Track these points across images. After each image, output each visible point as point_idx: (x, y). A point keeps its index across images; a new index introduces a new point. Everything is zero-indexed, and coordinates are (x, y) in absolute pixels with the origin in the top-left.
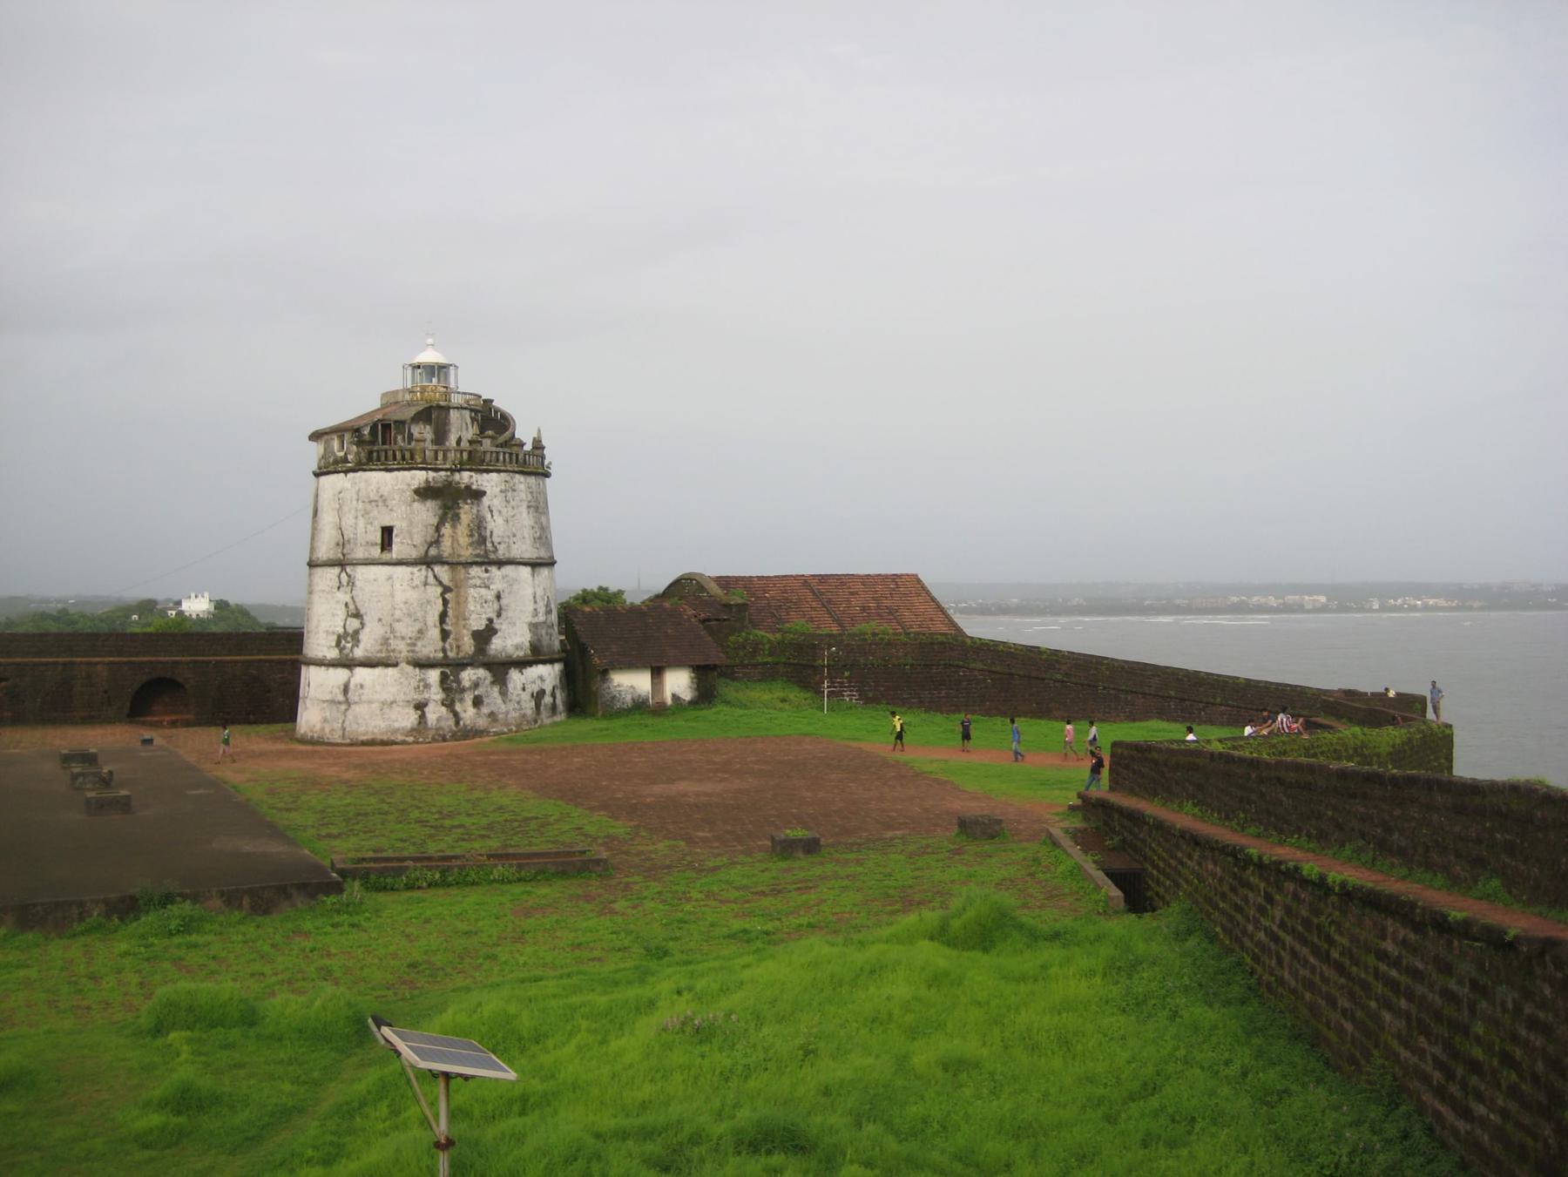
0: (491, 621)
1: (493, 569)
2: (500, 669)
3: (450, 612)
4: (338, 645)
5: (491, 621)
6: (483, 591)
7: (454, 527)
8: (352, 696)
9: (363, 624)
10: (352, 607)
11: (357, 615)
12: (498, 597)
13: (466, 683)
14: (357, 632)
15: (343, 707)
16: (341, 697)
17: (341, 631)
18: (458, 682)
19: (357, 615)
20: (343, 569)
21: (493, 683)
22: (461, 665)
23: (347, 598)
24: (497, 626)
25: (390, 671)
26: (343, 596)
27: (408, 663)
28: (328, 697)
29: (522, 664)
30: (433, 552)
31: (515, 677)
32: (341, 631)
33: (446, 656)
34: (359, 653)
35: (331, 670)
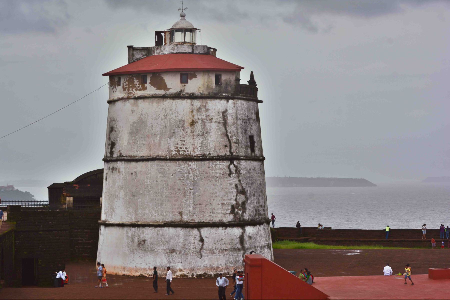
4: (233, 212)
8: (247, 245)
9: (247, 199)
10: (240, 188)
11: (243, 192)
14: (244, 204)
15: (242, 252)
16: (239, 246)
17: (234, 203)
19: (243, 192)
20: (232, 163)
23: (237, 182)
25: (262, 228)
26: (234, 180)
28: (229, 247)
32: (234, 203)
34: (246, 217)
35: (229, 230)
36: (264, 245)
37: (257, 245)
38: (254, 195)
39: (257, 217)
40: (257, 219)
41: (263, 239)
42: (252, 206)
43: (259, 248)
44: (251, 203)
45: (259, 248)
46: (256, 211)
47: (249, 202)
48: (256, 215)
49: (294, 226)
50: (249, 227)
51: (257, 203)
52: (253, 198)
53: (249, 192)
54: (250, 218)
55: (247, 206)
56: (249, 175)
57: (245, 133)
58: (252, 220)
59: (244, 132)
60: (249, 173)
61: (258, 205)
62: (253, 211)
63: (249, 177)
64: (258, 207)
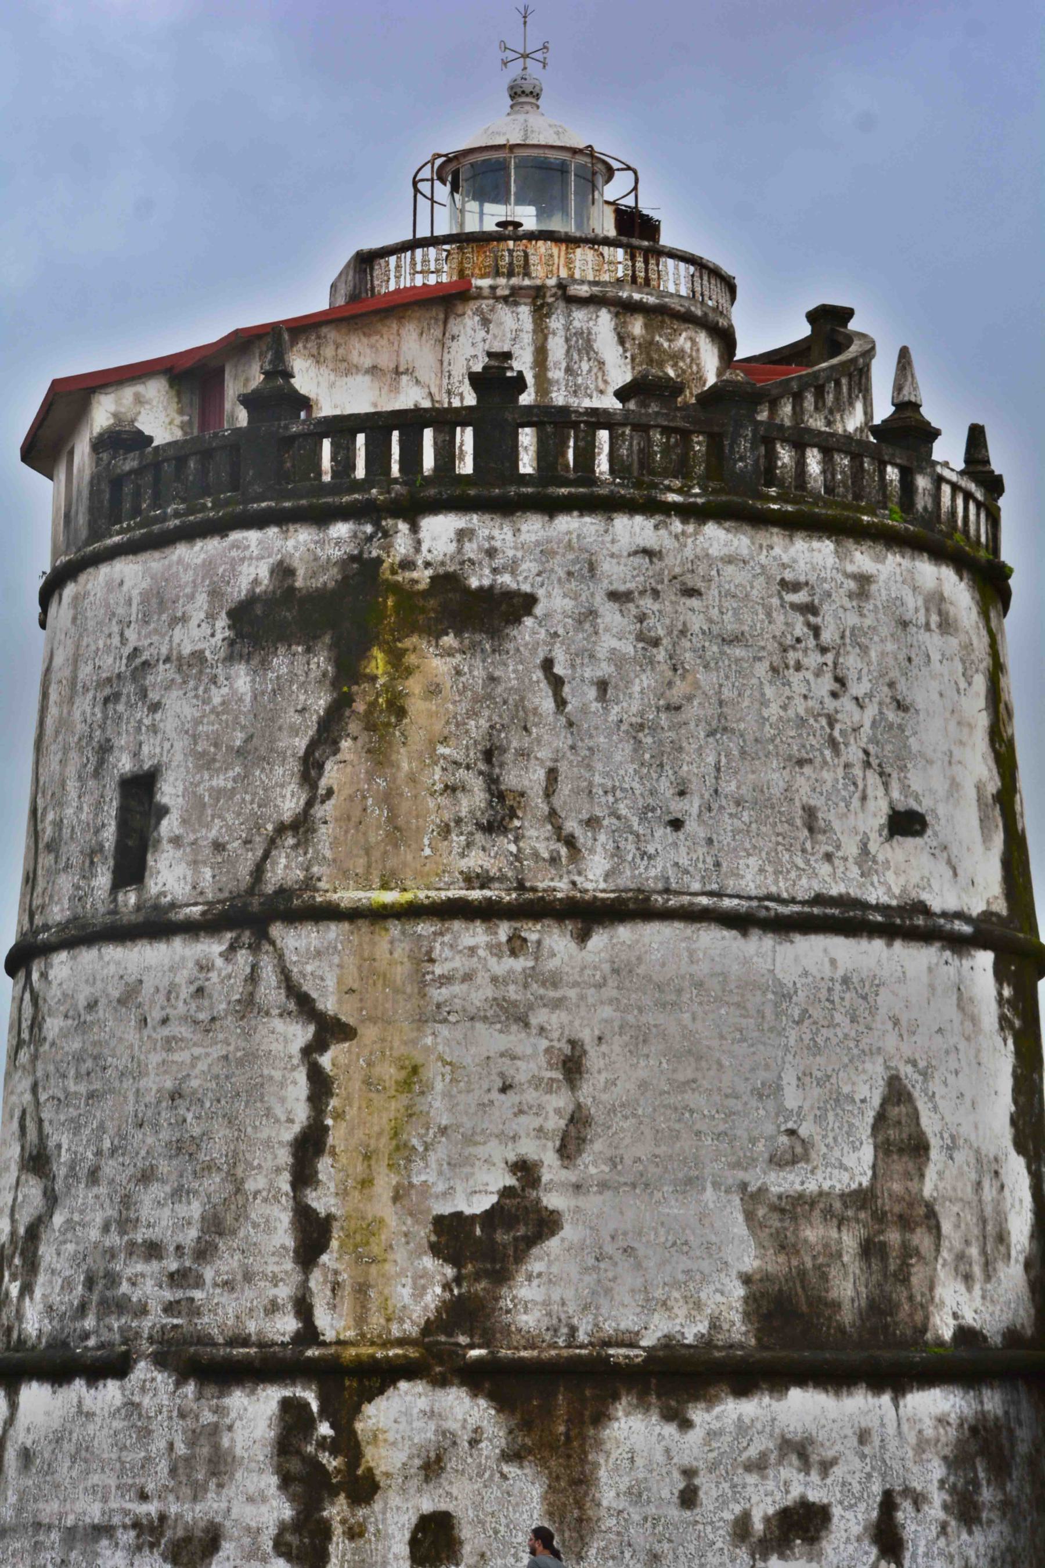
0: (526, 1171)
1: (557, 942)
2: (555, 1399)
3: (337, 1136)
5: (526, 1171)
6: (492, 1040)
7: (379, 756)
9: (52, 1200)
12: (572, 1066)
13: (385, 1458)
18: (347, 1443)
21: (513, 1455)
22: (380, 1376)
24: (552, 1200)
27: (160, 1361)
29: (678, 1378)
30: (284, 869)
31: (632, 1432)
33: (309, 1334)
36: (95, 1513)
37: (49, 1509)
38: (94, 1176)
39: (89, 1323)
40: (86, 1336)
41: (95, 1479)
42: (70, 1247)
43: (55, 1536)
44: (70, 1225)
45: (55, 1536)
46: (90, 1283)
47: (58, 1219)
48: (82, 1309)
49: (698, 1414)
50: (35, 1385)
51: (106, 1229)
52: (83, 1194)
53: (65, 1156)
54: (48, 1328)
55: (46, 1252)
56: (76, 1045)
57: (97, 774)
58: (58, 1344)
59: (90, 768)
60: (83, 1027)
61: (114, 1239)
62: (68, 1285)
63: (79, 1059)
64: (111, 1254)
